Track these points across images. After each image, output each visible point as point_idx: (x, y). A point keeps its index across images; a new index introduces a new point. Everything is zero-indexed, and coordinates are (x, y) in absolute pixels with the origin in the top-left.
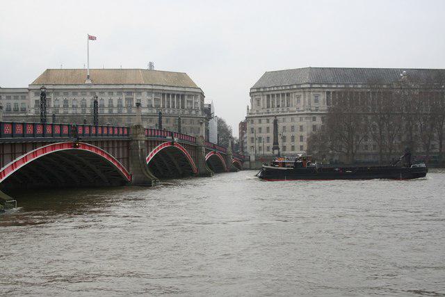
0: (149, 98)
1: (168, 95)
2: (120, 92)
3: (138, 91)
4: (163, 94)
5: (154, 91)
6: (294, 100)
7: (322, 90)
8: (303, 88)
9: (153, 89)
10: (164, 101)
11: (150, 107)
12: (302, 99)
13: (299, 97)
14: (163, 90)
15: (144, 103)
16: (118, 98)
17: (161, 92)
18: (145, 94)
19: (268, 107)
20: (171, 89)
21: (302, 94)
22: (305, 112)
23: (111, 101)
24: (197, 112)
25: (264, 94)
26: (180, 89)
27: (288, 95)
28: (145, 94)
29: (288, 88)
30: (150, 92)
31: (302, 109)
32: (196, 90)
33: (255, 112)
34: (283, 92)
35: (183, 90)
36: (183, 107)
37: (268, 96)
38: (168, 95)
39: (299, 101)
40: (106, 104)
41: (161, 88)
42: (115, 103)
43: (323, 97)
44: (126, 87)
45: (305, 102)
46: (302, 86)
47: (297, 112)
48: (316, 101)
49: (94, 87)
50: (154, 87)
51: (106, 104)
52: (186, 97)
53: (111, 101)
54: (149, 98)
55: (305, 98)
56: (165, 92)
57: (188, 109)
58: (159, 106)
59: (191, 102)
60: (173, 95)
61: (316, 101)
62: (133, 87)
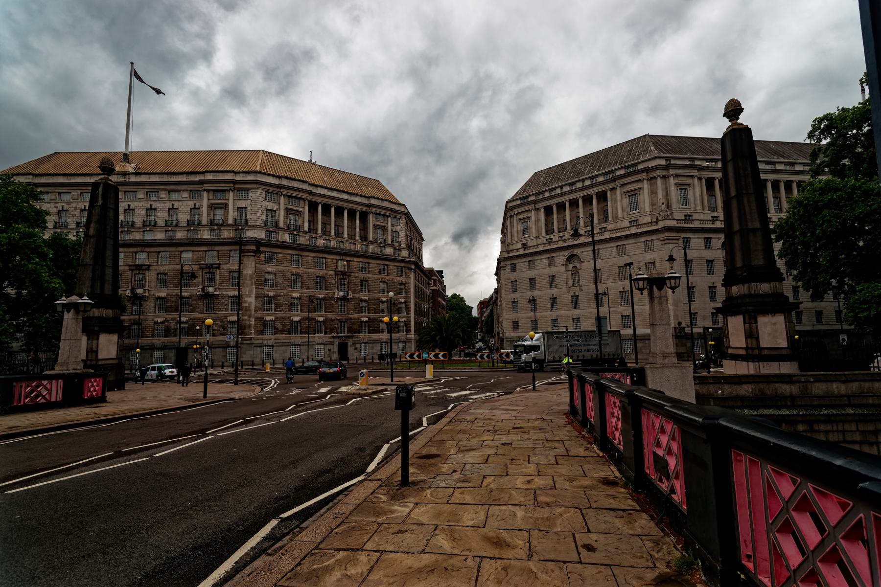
0: (270, 205)
1: (326, 209)
2: (196, 188)
3: (241, 187)
4: (313, 206)
5: (283, 191)
6: (618, 202)
7: (695, 172)
8: (647, 170)
9: (280, 187)
10: (312, 221)
11: (272, 226)
12: (645, 198)
13: (633, 194)
14: (311, 193)
15: (256, 216)
16: (191, 204)
17: (306, 196)
18: (258, 194)
19: (549, 231)
20: (334, 194)
21: (645, 185)
22: (661, 225)
23: (172, 210)
24: (397, 250)
25: (539, 206)
26: (357, 199)
27: (602, 197)
28: (258, 194)
29: (601, 179)
30: (273, 191)
31: (648, 219)
32: (396, 207)
33: (519, 246)
34: (586, 193)
35: (365, 201)
36: (364, 238)
37: (548, 211)
38: (326, 209)
39: (634, 205)
40: (139, 217)
41: (306, 187)
42: (183, 217)
43: (697, 191)
44: (209, 177)
45: (653, 204)
46: (640, 167)
47: (634, 230)
48: (685, 200)
49: (133, 179)
50: (285, 182)
51: (139, 217)
52: (371, 219)
53: (172, 210)
54: (270, 205)
55: (653, 192)
56: (319, 200)
57: (375, 242)
58: (298, 228)
59: (384, 229)
60: (339, 211)
61: (685, 200)
62: (229, 177)
